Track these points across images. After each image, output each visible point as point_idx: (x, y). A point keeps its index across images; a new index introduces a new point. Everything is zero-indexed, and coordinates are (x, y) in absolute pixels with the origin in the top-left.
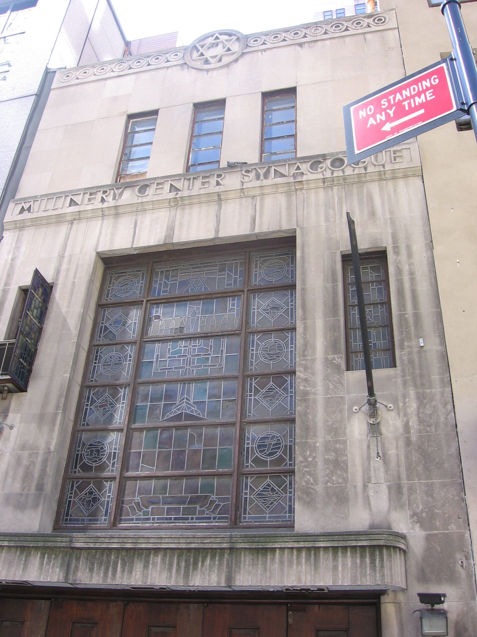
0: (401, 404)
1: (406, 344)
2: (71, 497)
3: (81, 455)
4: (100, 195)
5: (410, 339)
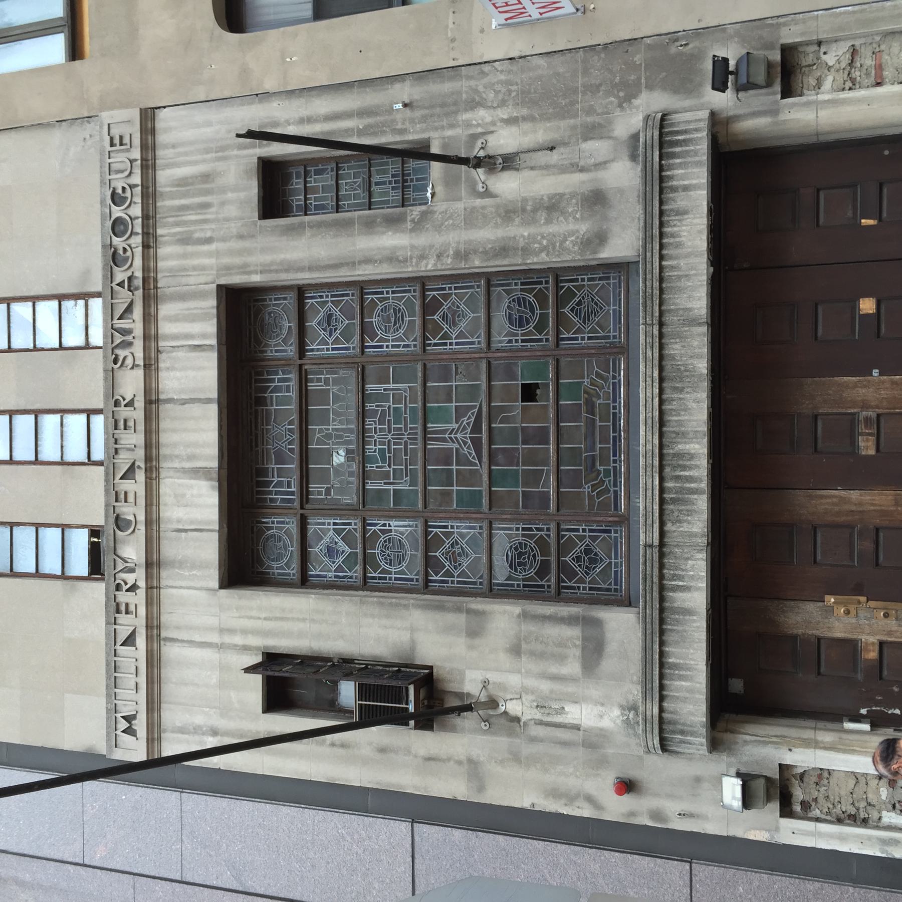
0: (480, 130)
1: (399, 126)
2: (584, 588)
3: (524, 580)
4: (123, 597)
5: (393, 121)
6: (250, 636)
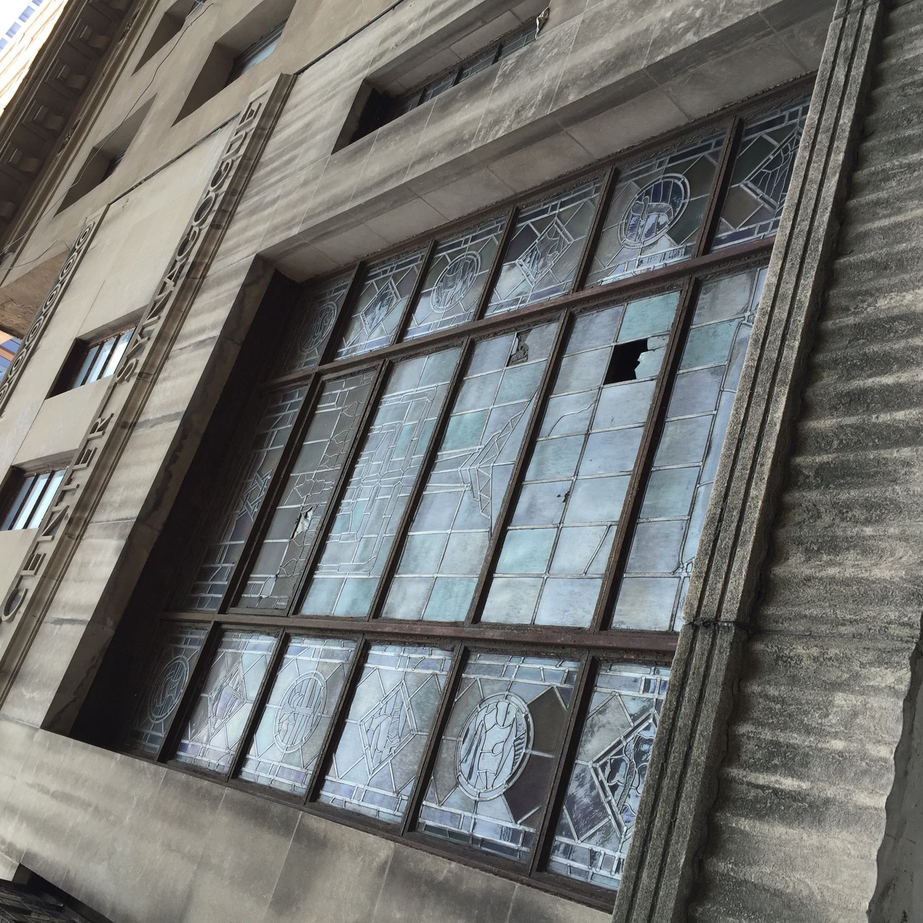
6: (25, 825)
